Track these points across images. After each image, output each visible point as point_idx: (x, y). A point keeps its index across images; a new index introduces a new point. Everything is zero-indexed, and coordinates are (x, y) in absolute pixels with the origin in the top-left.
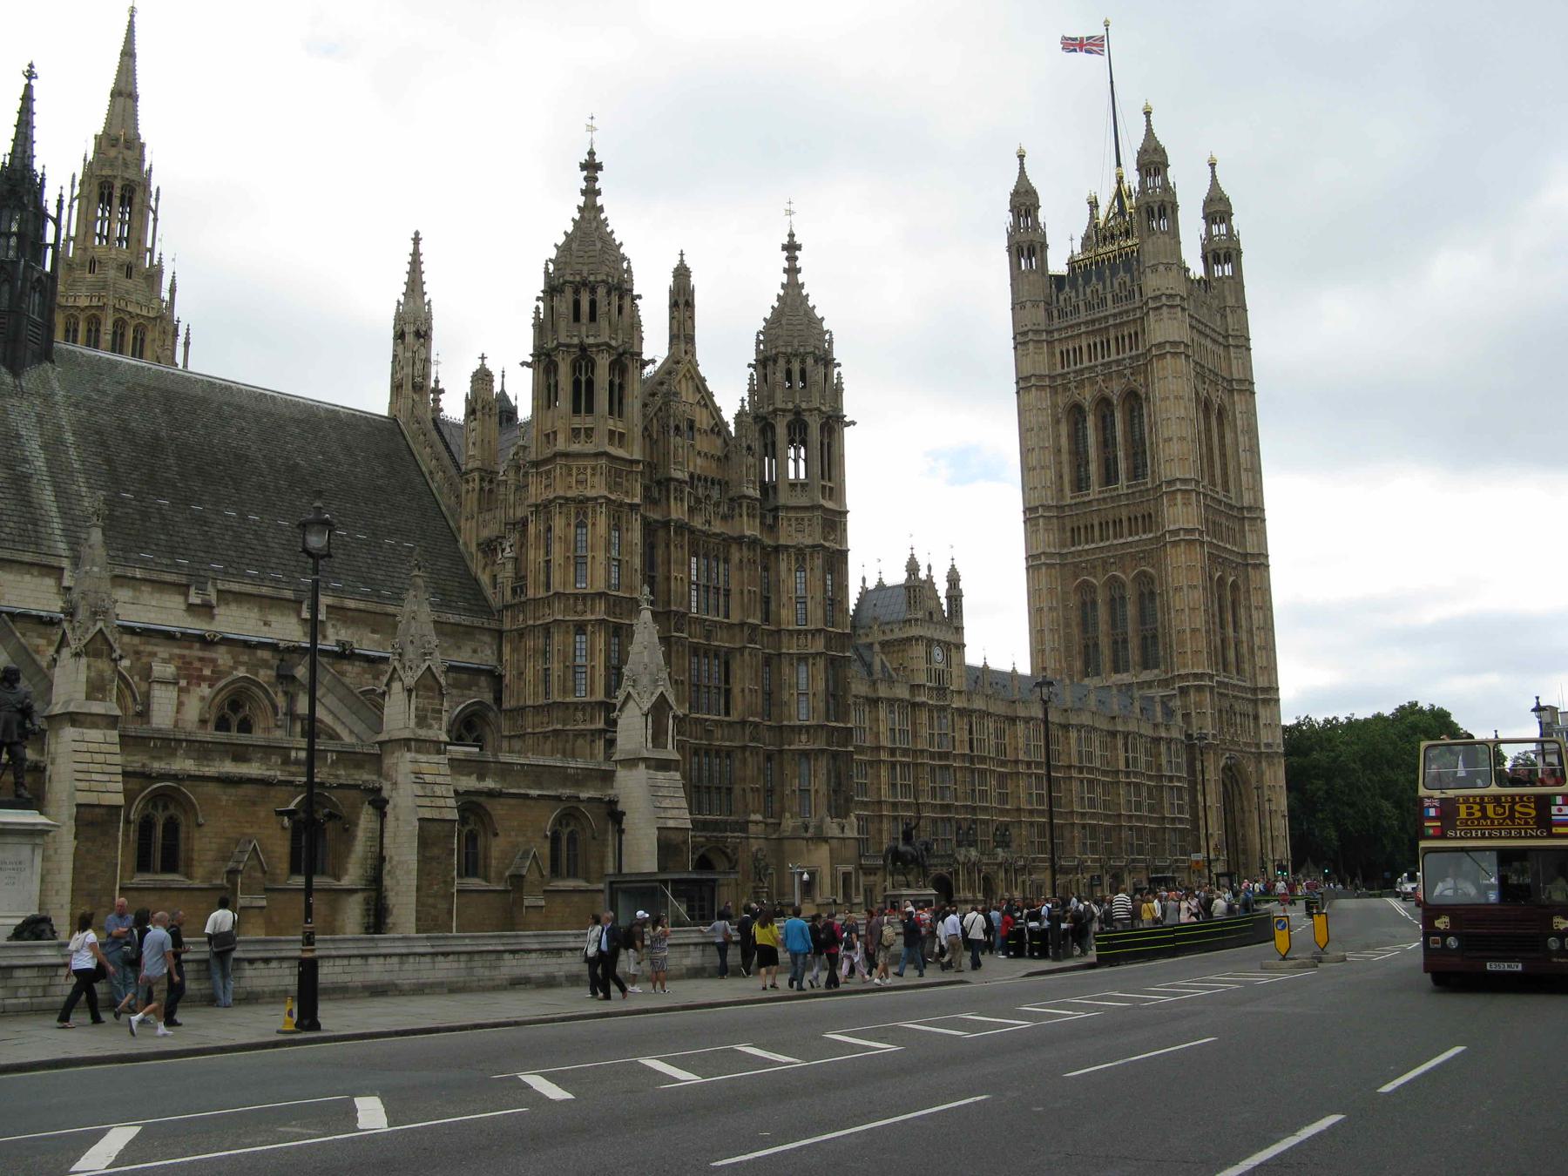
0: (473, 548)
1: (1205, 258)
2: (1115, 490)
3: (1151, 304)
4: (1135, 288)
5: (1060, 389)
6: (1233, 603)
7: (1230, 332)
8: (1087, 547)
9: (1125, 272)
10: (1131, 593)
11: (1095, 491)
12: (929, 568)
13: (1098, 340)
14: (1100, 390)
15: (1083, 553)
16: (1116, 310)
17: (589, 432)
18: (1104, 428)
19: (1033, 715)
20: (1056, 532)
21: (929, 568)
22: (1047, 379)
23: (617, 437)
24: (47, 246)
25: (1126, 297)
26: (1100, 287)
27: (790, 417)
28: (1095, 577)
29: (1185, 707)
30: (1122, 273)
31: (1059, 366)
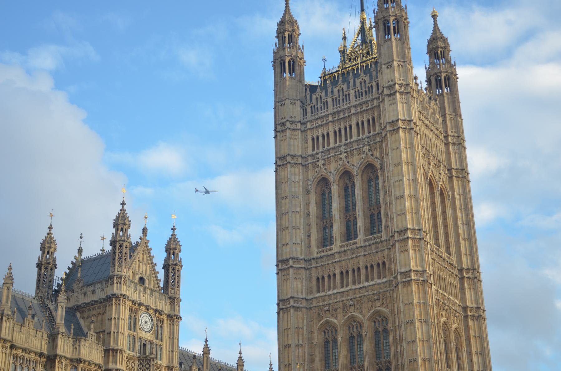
1: (429, 81)
2: (353, 244)
3: (386, 92)
5: (310, 166)
7: (450, 133)
8: (329, 293)
10: (367, 331)
11: (337, 245)
12: (145, 231)
14: (344, 165)
15: (327, 298)
16: (358, 103)
18: (346, 196)
20: (304, 281)
21: (145, 231)
25: (366, 92)
28: (336, 318)
30: (363, 75)
31: (310, 149)
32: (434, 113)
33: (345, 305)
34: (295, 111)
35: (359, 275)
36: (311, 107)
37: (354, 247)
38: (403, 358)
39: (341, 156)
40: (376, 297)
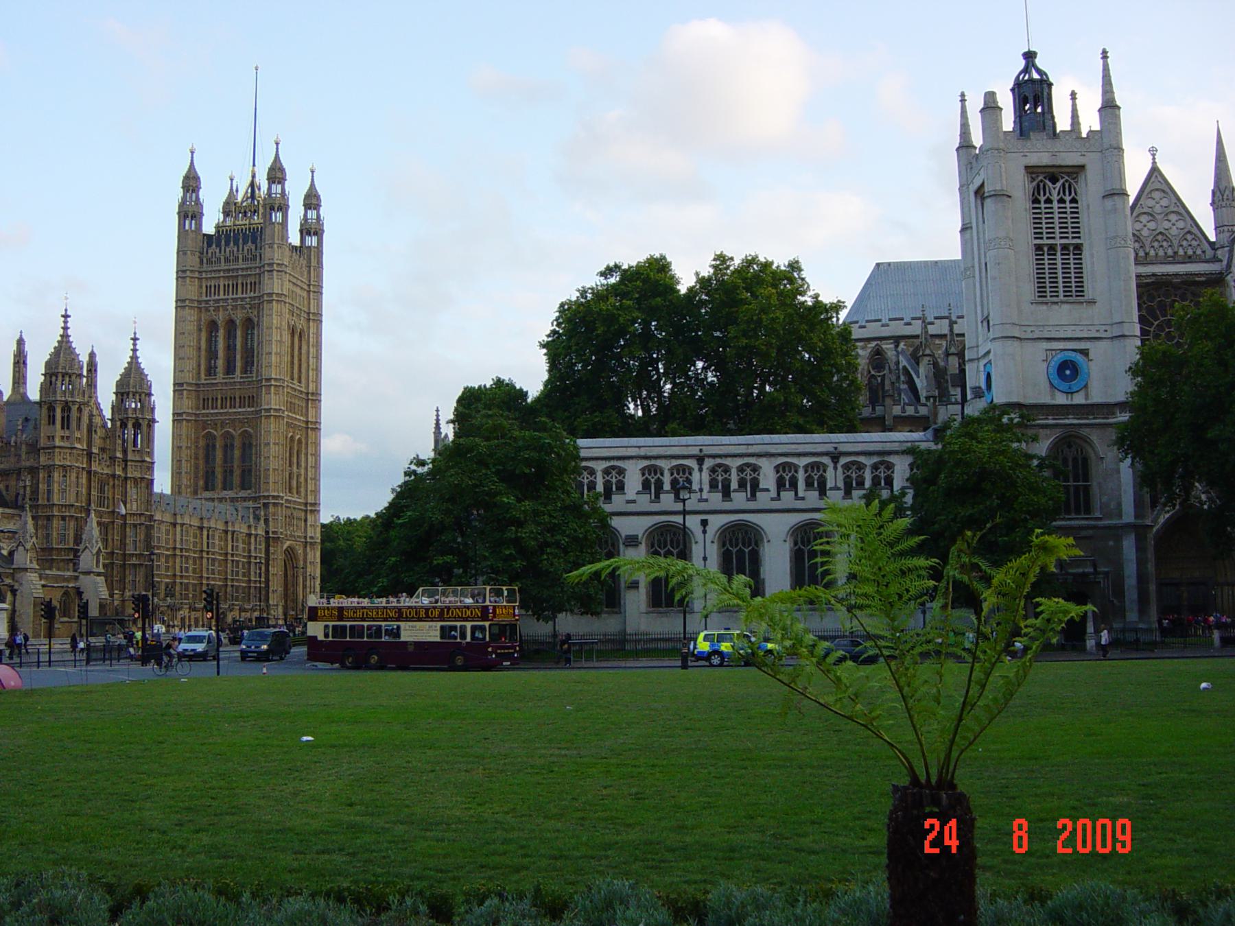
1: (301, 231)
3: (267, 268)
5: (203, 310)
6: (298, 451)
7: (312, 283)
8: (212, 411)
9: (253, 243)
10: (237, 443)
11: (220, 376)
13: (231, 283)
14: (229, 315)
18: (229, 338)
19: (185, 522)
23: (79, 440)
26: (235, 249)
27: (134, 421)
28: (216, 430)
29: (265, 515)
30: (250, 243)
31: (204, 295)
32: (301, 268)
33: (222, 422)
34: (193, 261)
38: (260, 466)
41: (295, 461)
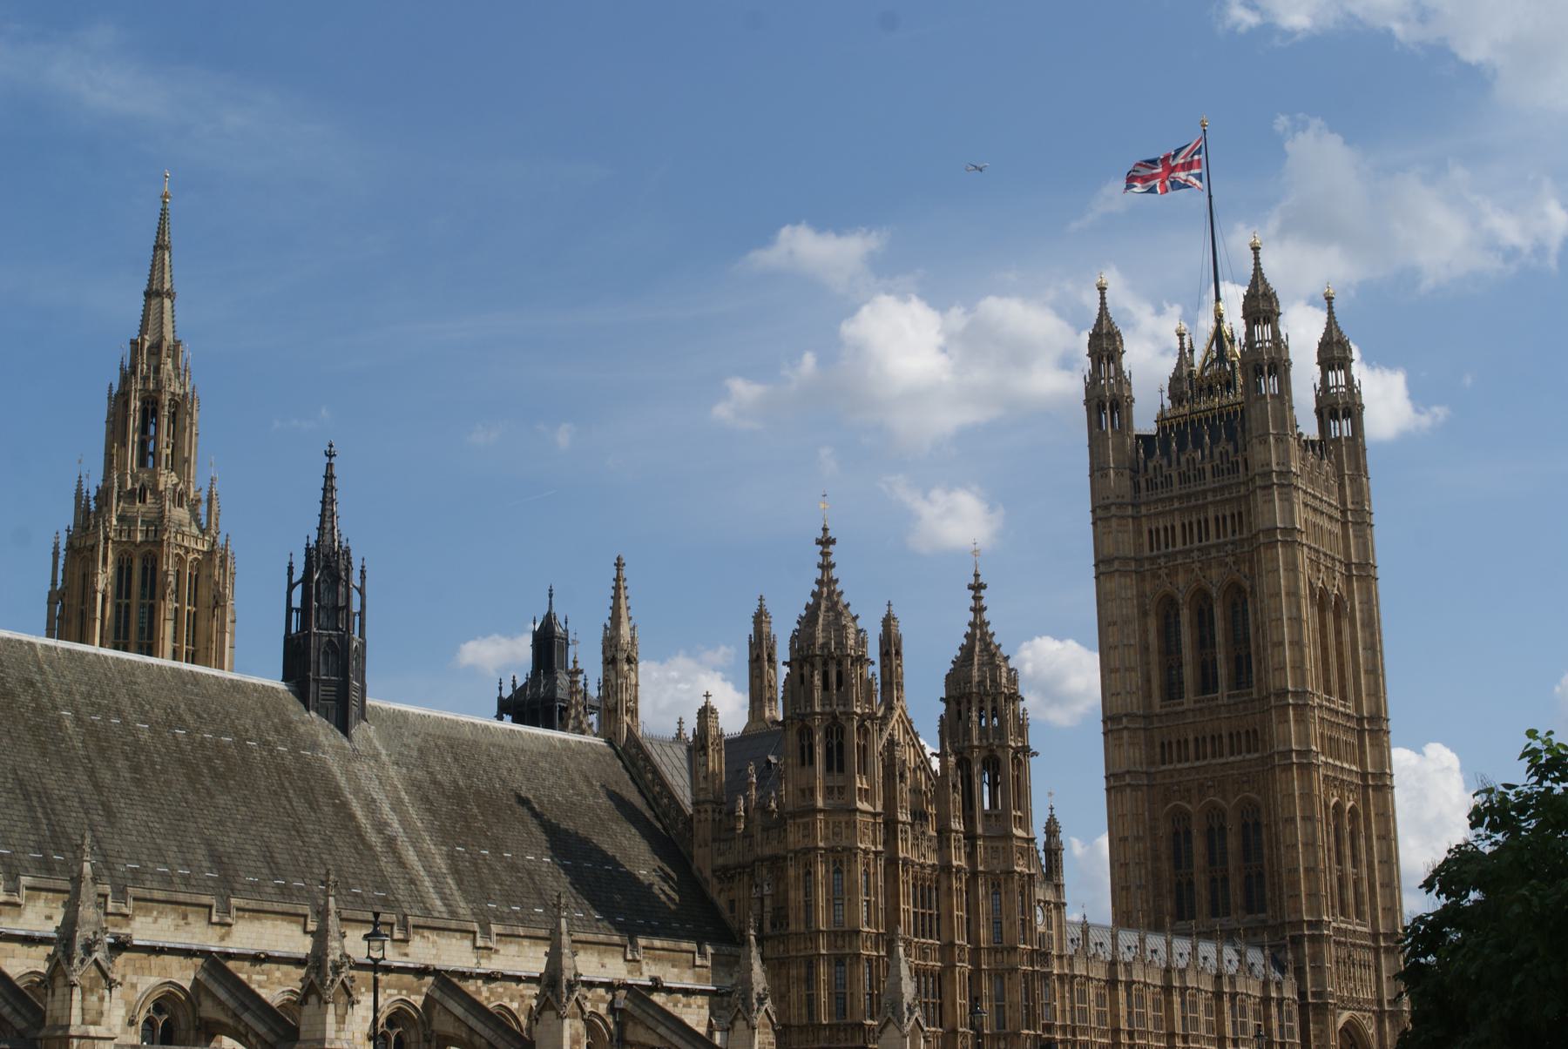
0: (708, 873)
1: (1319, 412)
2: (1213, 699)
4: (1240, 460)
6: (1352, 833)
7: (1350, 506)
8: (1179, 766)
10: (1233, 826)
11: (1189, 699)
13: (1194, 519)
16: (1216, 485)
17: (841, 790)
20: (1143, 747)
22: (1133, 564)
23: (867, 795)
24: (354, 615)
25: (1228, 469)
27: (985, 753)
28: (1190, 802)
32: (1327, 480)
35: (1221, 742)
36: (1147, 480)
37: (1214, 704)
39: (1193, 566)
40: (1245, 779)
41: (1348, 852)
